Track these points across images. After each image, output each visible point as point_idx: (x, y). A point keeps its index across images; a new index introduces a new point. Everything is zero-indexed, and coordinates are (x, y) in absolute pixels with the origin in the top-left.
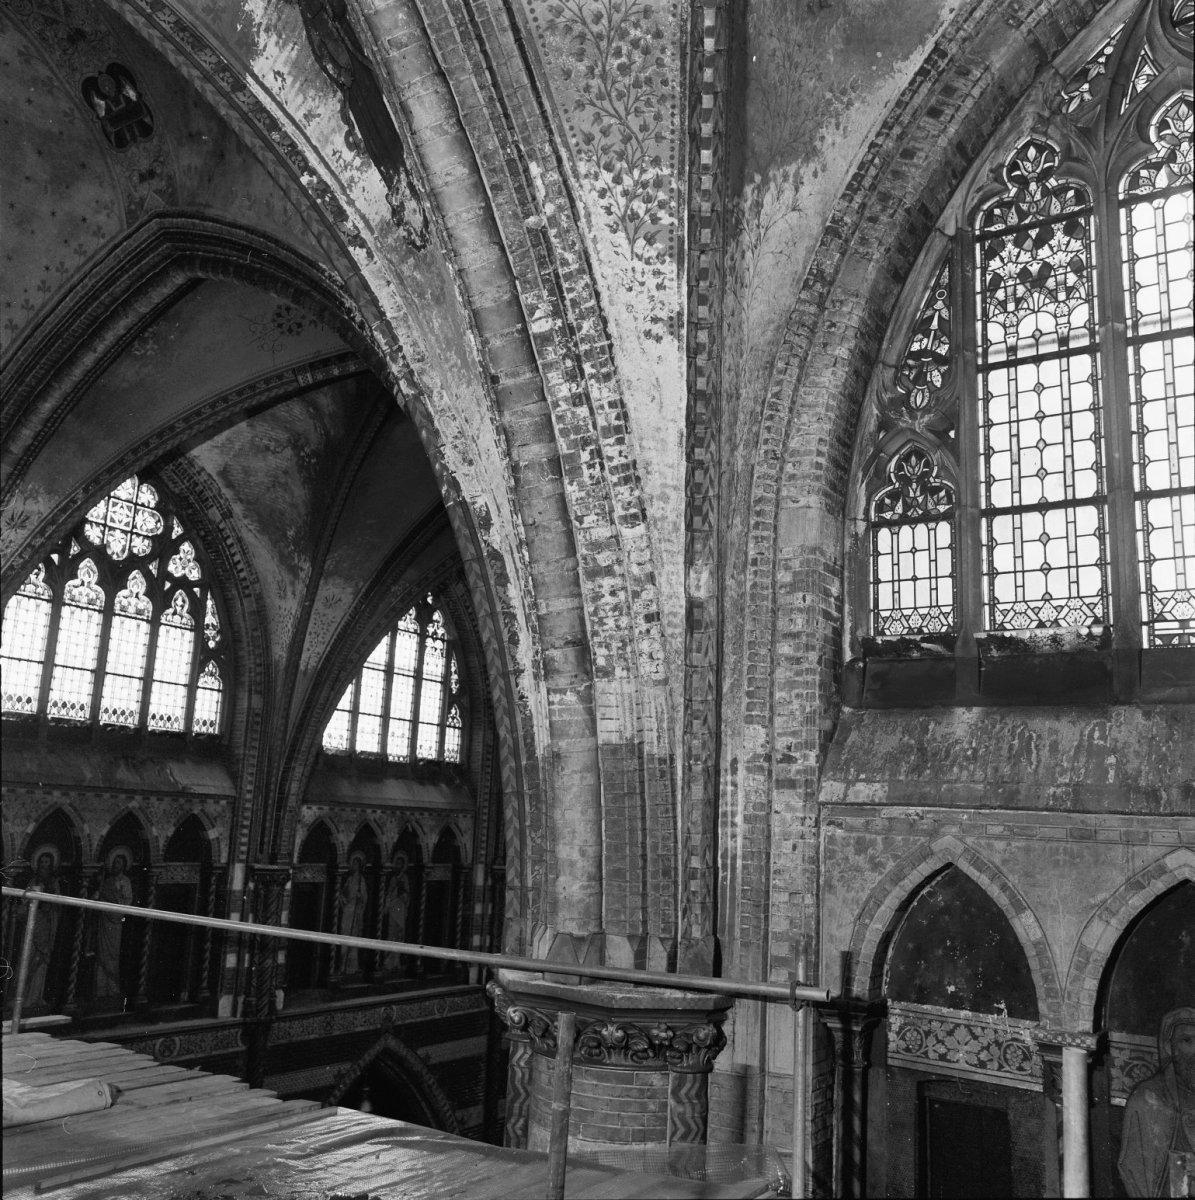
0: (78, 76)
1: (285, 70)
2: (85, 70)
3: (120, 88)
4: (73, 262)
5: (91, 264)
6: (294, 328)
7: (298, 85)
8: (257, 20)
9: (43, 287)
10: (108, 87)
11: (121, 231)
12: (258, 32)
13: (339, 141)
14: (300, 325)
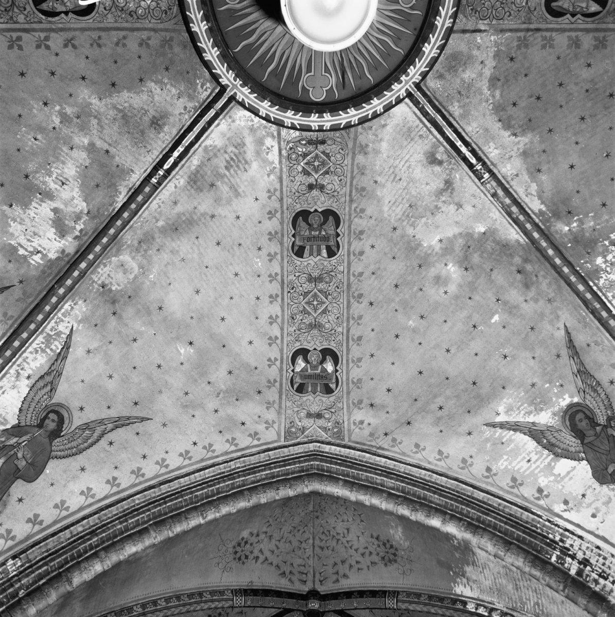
0: (298, 344)
2: (305, 343)
3: (323, 361)
4: (221, 446)
5: (239, 454)
6: (243, 558)
9: (185, 455)
10: (314, 358)
11: (275, 441)
14: (247, 557)
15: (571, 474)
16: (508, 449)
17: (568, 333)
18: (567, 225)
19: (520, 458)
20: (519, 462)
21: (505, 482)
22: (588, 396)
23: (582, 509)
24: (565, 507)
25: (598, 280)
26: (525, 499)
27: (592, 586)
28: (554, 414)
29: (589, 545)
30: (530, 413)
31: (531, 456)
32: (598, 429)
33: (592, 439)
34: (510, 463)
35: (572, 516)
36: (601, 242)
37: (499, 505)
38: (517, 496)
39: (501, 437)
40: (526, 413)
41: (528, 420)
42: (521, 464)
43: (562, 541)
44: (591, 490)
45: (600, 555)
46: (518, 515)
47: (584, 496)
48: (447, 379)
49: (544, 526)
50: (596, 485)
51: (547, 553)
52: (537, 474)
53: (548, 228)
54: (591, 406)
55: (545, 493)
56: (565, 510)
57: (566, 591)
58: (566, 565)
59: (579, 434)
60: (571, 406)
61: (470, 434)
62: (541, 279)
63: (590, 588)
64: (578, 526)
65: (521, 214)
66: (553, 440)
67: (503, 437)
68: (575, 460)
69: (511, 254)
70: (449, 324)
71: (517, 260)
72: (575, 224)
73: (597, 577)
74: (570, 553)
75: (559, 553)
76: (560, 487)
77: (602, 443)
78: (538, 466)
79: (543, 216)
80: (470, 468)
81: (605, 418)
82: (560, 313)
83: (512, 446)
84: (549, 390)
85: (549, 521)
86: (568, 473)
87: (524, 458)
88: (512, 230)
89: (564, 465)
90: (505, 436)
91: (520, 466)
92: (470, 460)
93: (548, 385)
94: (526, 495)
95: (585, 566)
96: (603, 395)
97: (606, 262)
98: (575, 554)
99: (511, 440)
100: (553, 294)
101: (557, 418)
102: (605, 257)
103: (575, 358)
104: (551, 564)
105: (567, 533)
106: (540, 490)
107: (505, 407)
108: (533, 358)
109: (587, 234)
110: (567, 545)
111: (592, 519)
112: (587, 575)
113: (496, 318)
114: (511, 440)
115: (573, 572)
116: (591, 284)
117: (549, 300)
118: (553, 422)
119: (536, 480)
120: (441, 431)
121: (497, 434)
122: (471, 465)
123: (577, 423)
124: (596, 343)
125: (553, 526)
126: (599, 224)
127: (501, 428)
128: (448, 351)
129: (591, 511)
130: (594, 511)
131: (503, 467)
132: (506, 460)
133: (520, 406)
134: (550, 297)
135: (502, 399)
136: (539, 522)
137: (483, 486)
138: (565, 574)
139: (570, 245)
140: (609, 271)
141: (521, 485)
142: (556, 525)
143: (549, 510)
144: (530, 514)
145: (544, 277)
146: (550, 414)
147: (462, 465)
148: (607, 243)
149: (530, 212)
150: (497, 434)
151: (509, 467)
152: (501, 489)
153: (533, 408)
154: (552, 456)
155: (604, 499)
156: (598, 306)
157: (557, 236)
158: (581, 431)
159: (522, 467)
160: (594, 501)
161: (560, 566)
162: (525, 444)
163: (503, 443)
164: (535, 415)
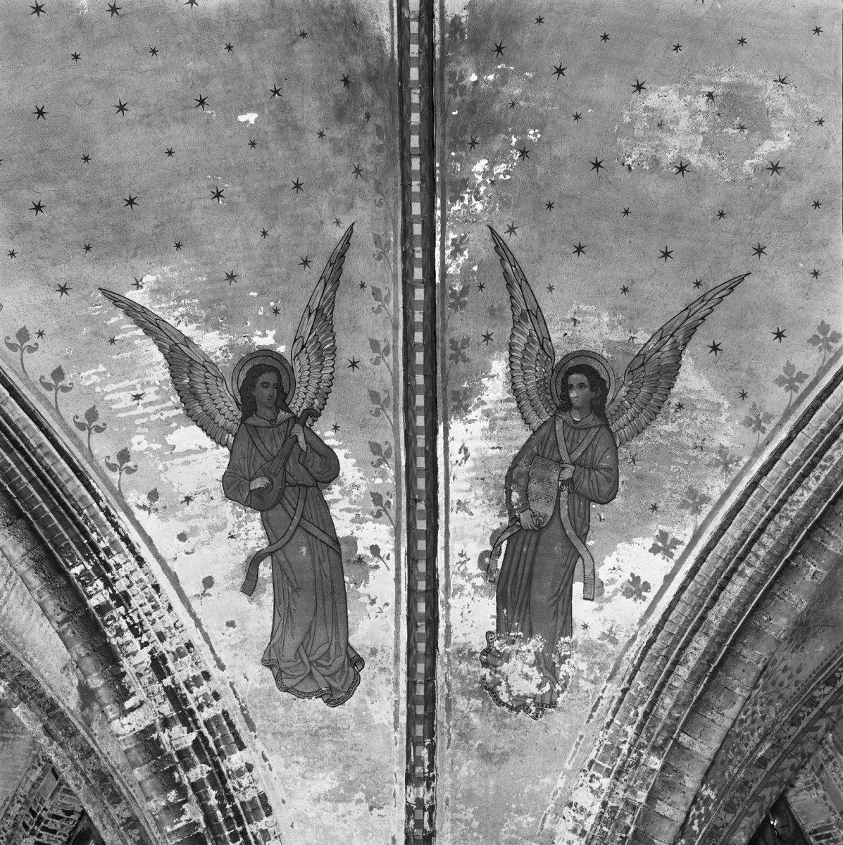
1: (473, 454)
7: (473, 474)
8: (484, 398)
12: (477, 406)
13: (475, 550)
15: (193, 457)
16: (115, 357)
17: (347, 240)
18: (478, 72)
19: (127, 383)
20: (119, 390)
21: (72, 409)
22: (303, 357)
23: (172, 519)
24: (147, 503)
25: (453, 201)
26: (90, 456)
27: (109, 634)
28: (231, 347)
29: (145, 578)
30: (193, 319)
31: (147, 390)
32: (283, 415)
33: (263, 423)
34: (103, 384)
35: (150, 522)
36: (507, 133)
37: (40, 446)
38: (80, 446)
39: (116, 329)
40: (188, 314)
41: (181, 327)
42: (121, 395)
43: (107, 551)
44: (205, 497)
45: (151, 599)
46: (62, 479)
47: (188, 499)
48: (86, 159)
49: (94, 516)
50: (218, 494)
51: (71, 558)
52: (136, 426)
53: (444, 60)
54: (297, 375)
55: (130, 464)
56: (144, 507)
57: (65, 626)
58: (89, 589)
59: (248, 404)
60: (267, 353)
61: (63, 290)
62: (370, 127)
63: (105, 636)
64: (149, 541)
65: (419, 19)
66: (200, 388)
67: (120, 331)
68: (213, 438)
69: (354, 45)
70: (158, 61)
71: (357, 63)
72: (491, 77)
73: (125, 626)
74: (109, 575)
75: (90, 568)
76: (161, 467)
77: (273, 438)
78: (147, 415)
79: (452, 34)
80: (26, 354)
81: (305, 407)
82: (359, 202)
83: (127, 354)
84: (251, 303)
85: (107, 513)
86: (189, 452)
87: (134, 388)
88: (387, 18)
89: (190, 436)
90: (125, 331)
91: (118, 397)
92: (34, 339)
93: (255, 294)
94: (95, 452)
95: (118, 605)
96: (326, 372)
97: (486, 174)
98: (115, 581)
99: (129, 344)
100: (370, 167)
101: (231, 356)
102: (492, 164)
103: (329, 287)
104: (66, 576)
105: (123, 545)
106: (124, 455)
107: (157, 282)
108: (264, 233)
109: (497, 107)
110: (111, 562)
111: (177, 541)
112: (113, 618)
113: (251, 117)
114: (129, 344)
115: (93, 603)
116: (438, 202)
117: (358, 171)
118: (222, 358)
119: (130, 434)
120: (12, 254)
121: (114, 320)
122: (31, 349)
123: (258, 385)
124: (376, 293)
125: (108, 524)
126: (527, 99)
127: (127, 313)
128: (122, 108)
129: (183, 528)
130: (188, 530)
131: (88, 383)
132: (99, 374)
133: (186, 297)
134: (363, 166)
135: (162, 263)
136: (89, 507)
137: (31, 398)
138: (79, 600)
139: (455, 113)
140: (481, 193)
141: (99, 430)
142: (116, 526)
143: (119, 495)
144: (82, 488)
145: (379, 131)
146: (224, 342)
147: (14, 340)
148: (514, 140)
149: (437, 15)
150: (114, 320)
151: (98, 389)
152: (61, 420)
153: (204, 313)
154: (181, 411)
155: (215, 521)
156: (419, 255)
157: (448, 85)
158: (255, 402)
159: (119, 400)
160: (198, 516)
161: (79, 585)
162: (151, 365)
163: (112, 341)
164: (198, 328)
